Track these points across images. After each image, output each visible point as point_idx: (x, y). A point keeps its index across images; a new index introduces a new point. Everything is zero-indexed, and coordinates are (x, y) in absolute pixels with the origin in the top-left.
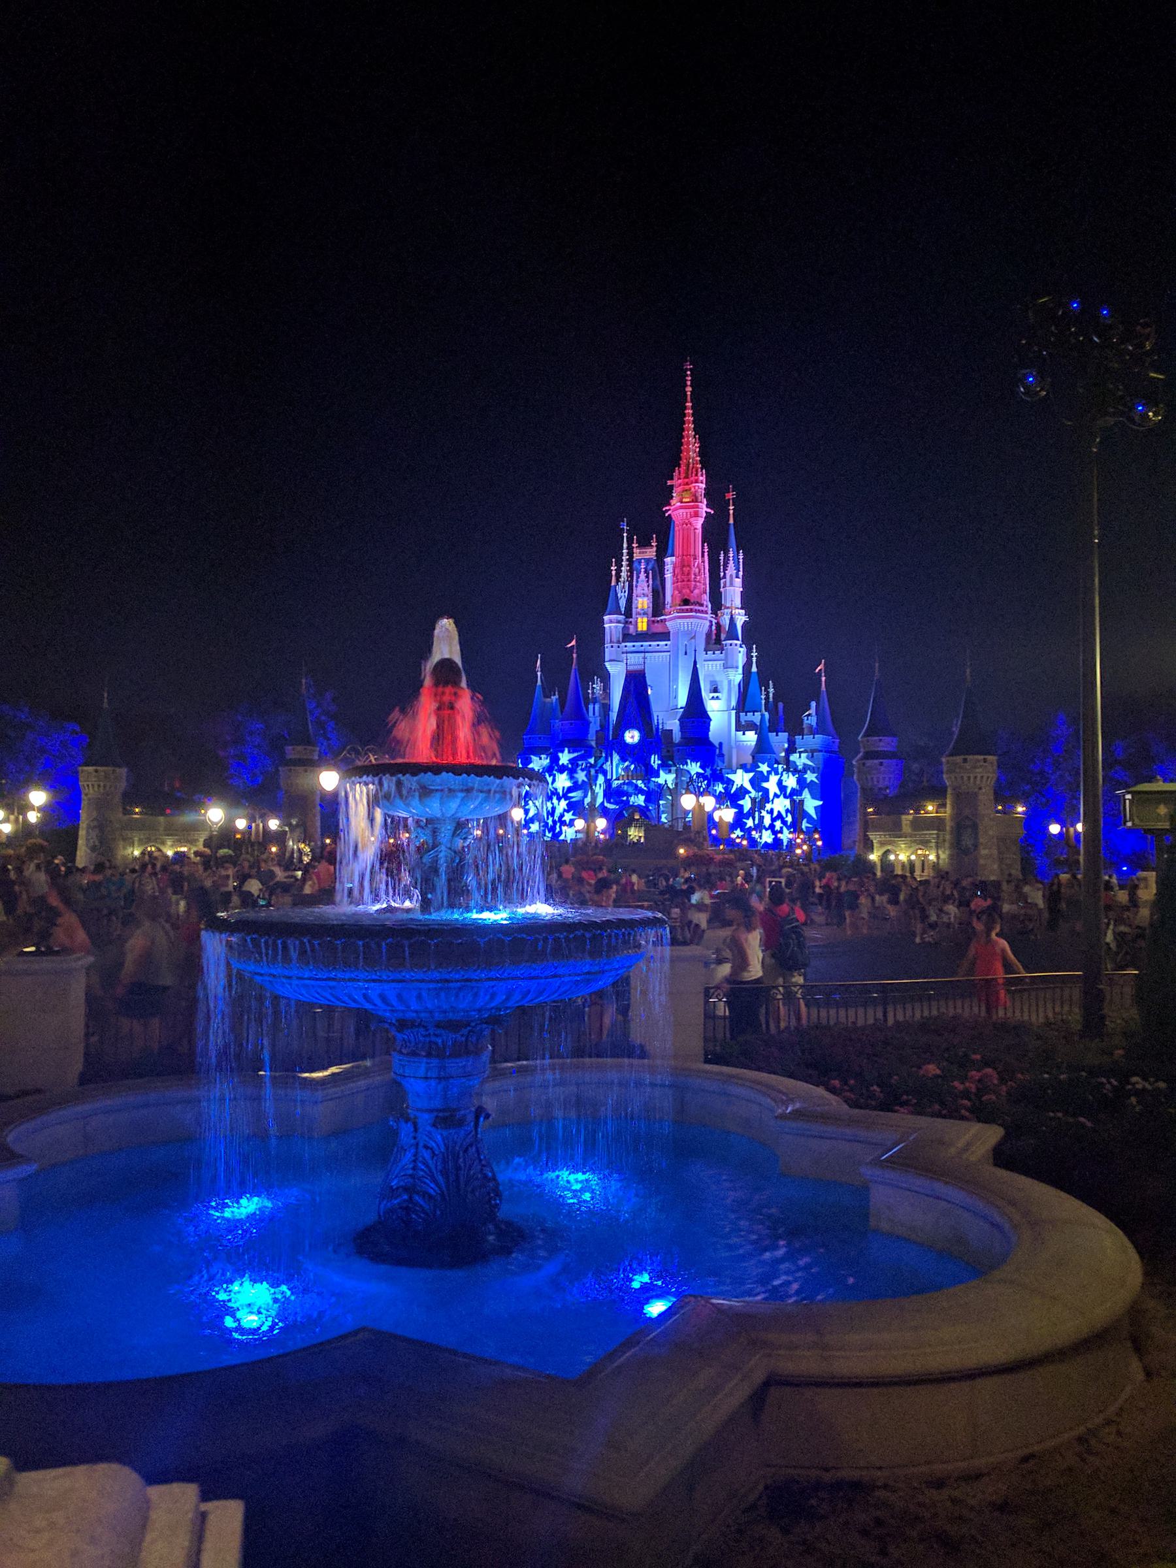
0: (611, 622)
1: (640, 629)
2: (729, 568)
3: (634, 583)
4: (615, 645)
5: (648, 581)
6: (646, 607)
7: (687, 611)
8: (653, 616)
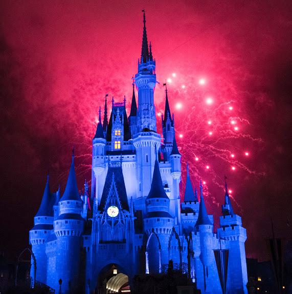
0: (98, 142)
1: (116, 148)
2: (167, 121)
3: (113, 121)
4: (100, 157)
5: (121, 120)
6: (119, 134)
7: (148, 135)
8: (124, 140)
